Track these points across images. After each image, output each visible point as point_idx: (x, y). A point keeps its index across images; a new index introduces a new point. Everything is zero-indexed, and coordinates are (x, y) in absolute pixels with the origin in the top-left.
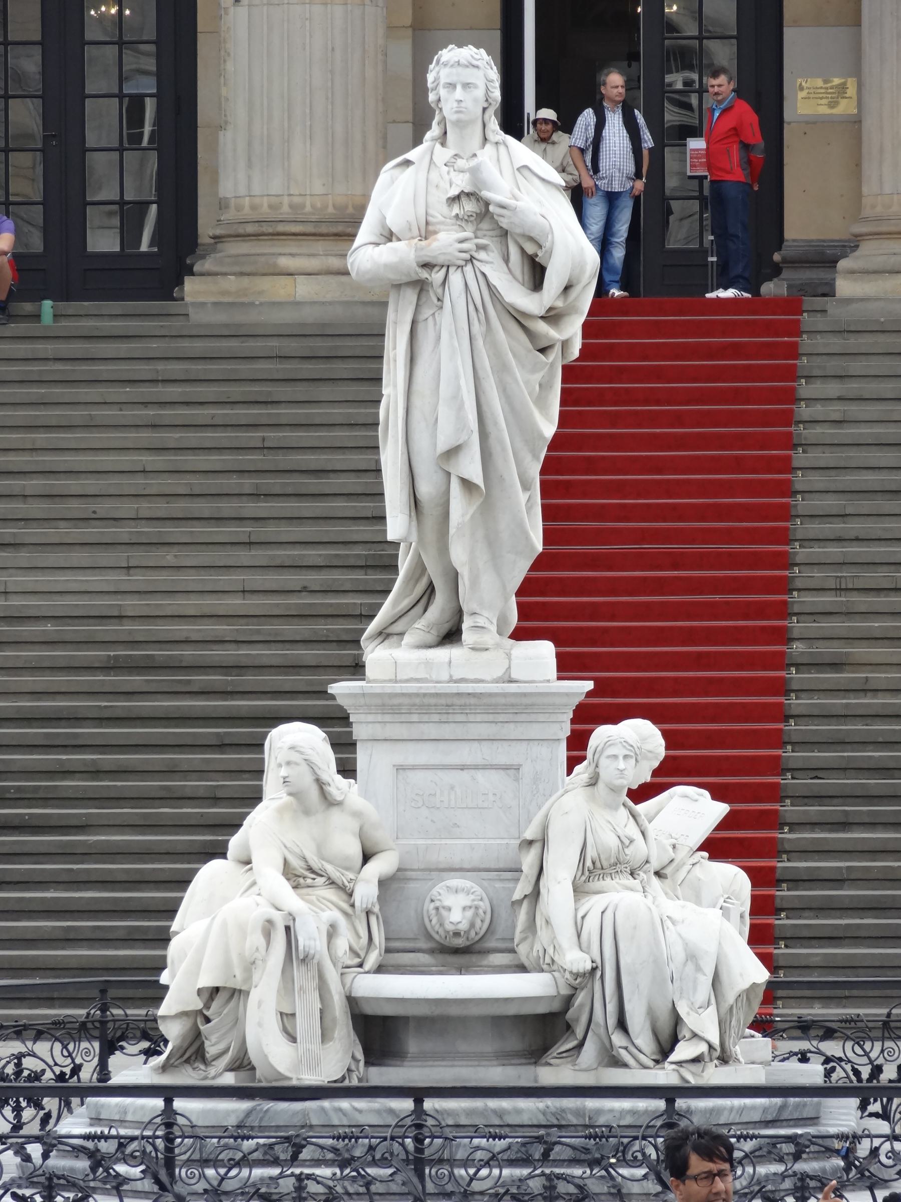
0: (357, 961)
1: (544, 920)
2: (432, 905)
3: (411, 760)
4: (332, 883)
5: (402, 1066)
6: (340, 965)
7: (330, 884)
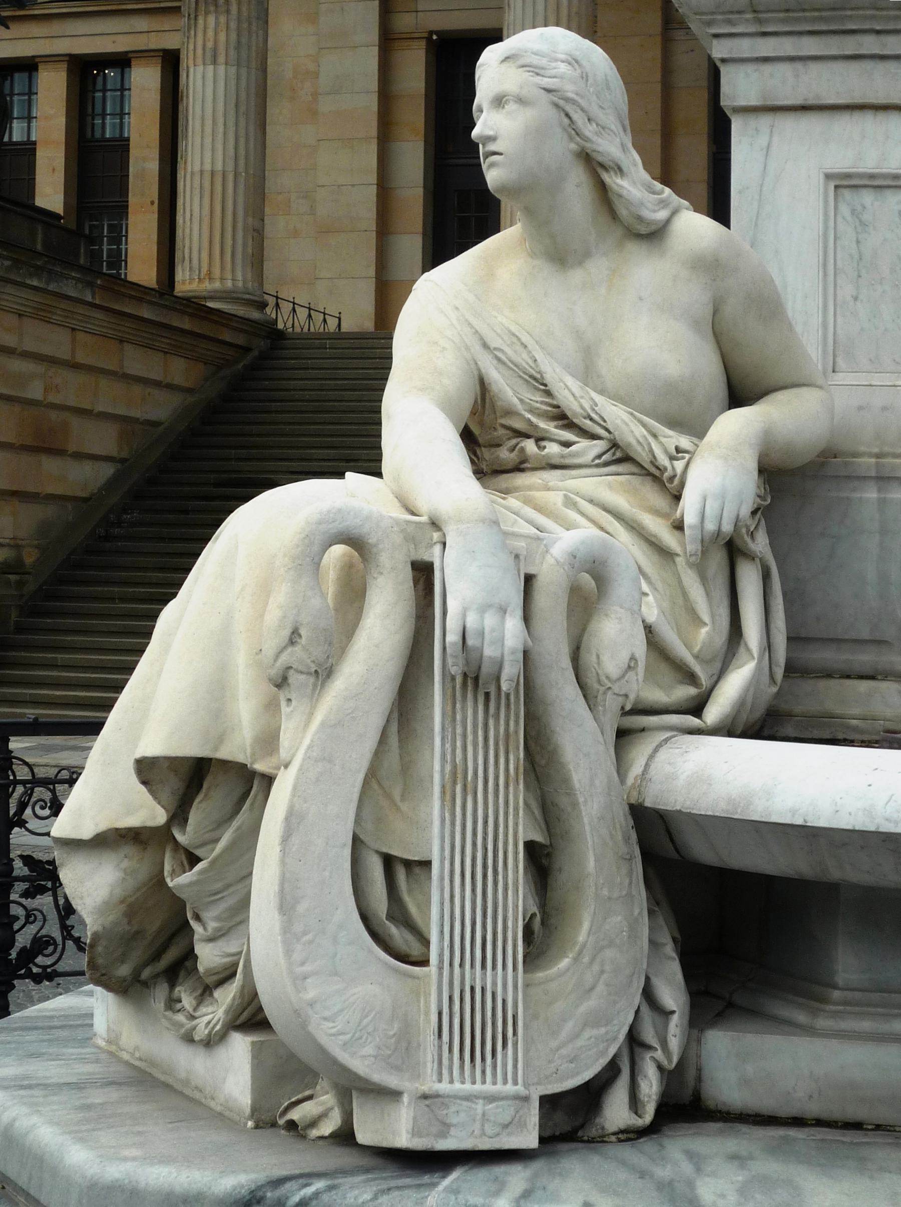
0: (684, 692)
3: (870, 163)
4: (620, 456)
5: (810, 1031)
6: (611, 705)
7: (619, 461)
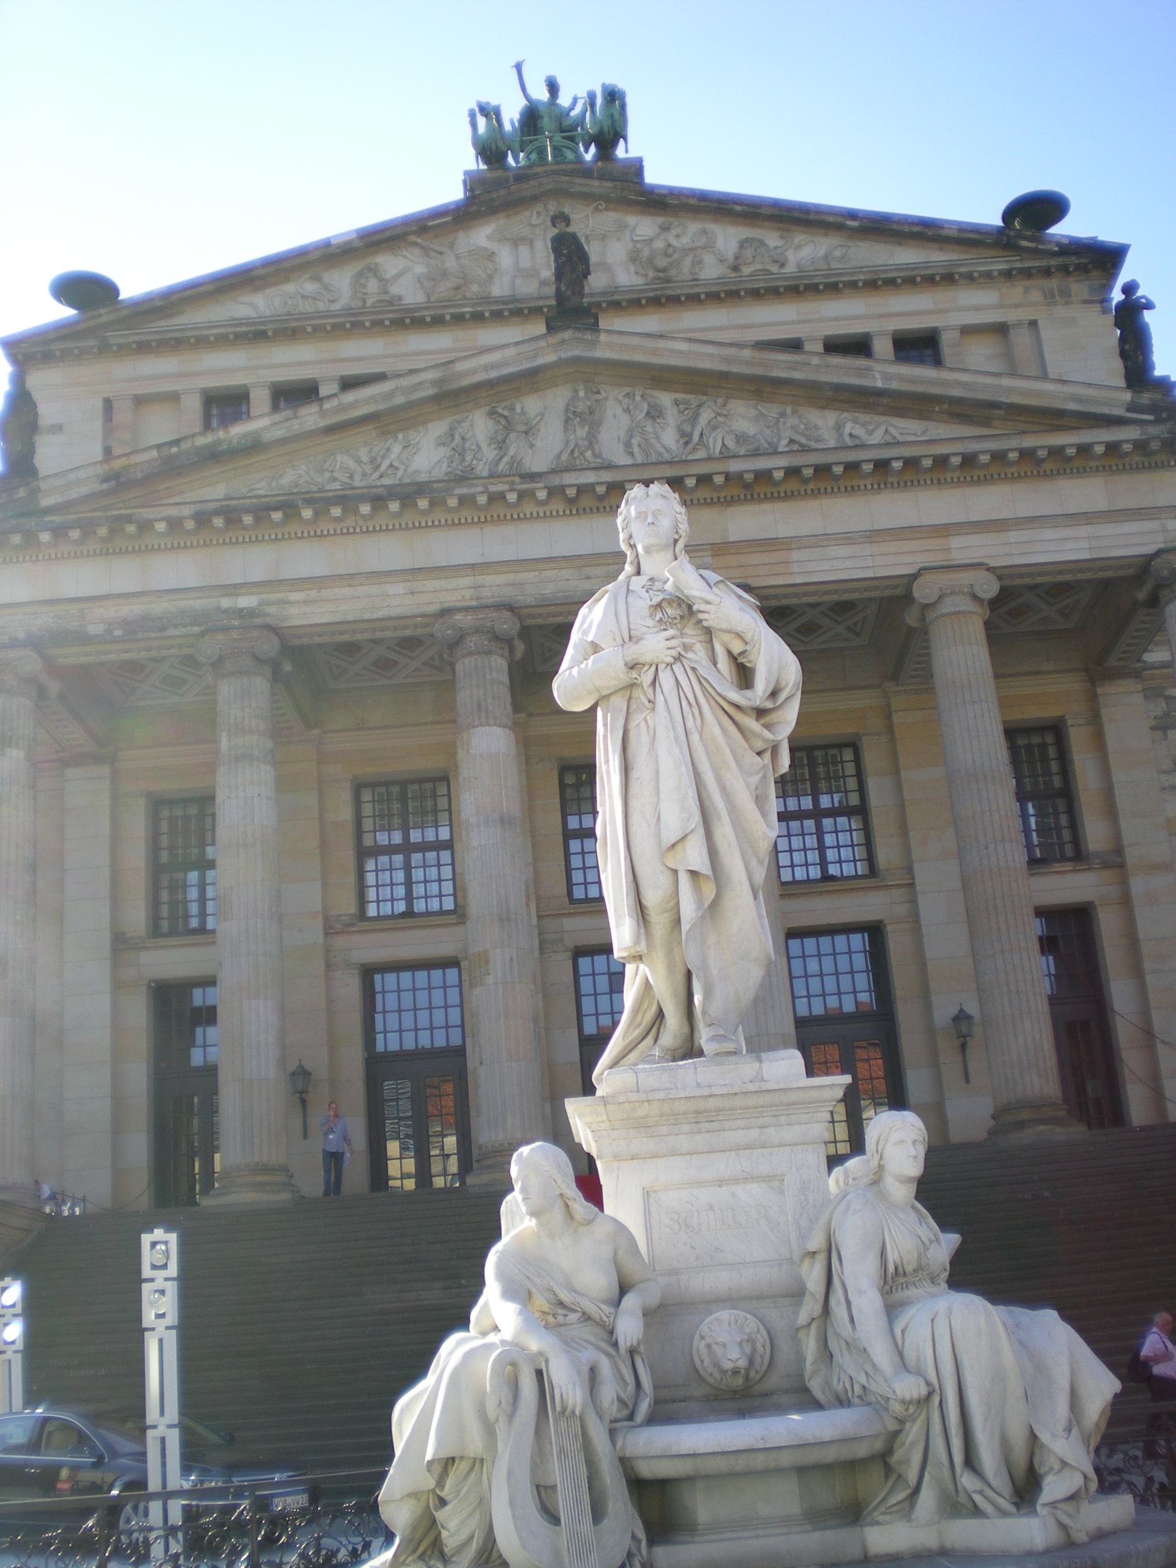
0: (626, 1412)
1: (843, 1344)
2: (703, 1343)
7: (586, 1320)
